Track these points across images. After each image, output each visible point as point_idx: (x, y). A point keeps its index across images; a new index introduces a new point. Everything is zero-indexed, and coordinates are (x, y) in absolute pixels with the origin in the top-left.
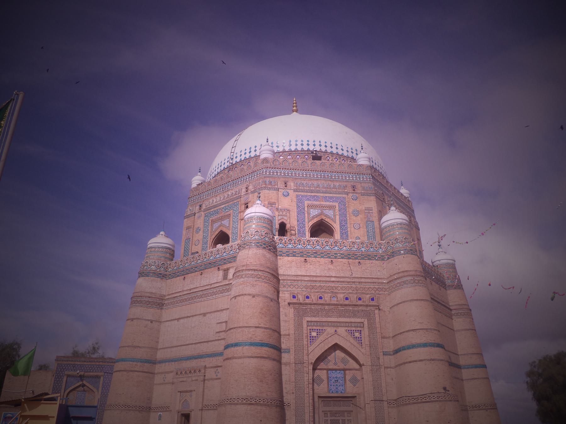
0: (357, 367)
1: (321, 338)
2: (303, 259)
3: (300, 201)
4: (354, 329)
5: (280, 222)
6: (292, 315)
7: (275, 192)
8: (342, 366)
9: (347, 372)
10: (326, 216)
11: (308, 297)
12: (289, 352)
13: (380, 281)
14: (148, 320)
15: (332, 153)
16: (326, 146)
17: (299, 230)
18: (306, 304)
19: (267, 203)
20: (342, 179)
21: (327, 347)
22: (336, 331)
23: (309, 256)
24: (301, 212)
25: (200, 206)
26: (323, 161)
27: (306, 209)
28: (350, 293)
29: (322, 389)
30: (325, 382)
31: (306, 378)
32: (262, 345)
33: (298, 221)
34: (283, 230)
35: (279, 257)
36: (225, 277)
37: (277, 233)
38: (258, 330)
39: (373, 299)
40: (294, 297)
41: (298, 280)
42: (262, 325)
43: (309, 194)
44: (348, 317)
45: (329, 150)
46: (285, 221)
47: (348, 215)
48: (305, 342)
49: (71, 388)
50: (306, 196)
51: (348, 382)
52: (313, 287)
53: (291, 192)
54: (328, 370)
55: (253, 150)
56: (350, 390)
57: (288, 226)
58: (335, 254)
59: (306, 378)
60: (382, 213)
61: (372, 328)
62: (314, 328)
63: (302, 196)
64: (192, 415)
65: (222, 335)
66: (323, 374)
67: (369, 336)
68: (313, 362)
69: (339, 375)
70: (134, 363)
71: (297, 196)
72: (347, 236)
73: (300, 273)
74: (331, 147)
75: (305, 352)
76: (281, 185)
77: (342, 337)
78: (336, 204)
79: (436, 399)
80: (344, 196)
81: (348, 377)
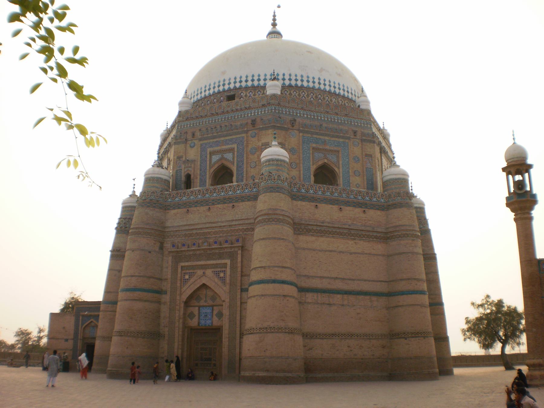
1: (192, 280)
2: (185, 210)
3: (203, 149)
4: (219, 269)
5: (186, 173)
6: (170, 263)
7: (183, 145)
8: (210, 302)
9: (215, 308)
10: (226, 159)
11: (184, 245)
12: (166, 293)
13: (249, 221)
14: (117, 270)
15: (247, 88)
17: (200, 179)
18: (182, 251)
19: (176, 157)
20: (244, 117)
21: (196, 287)
23: (190, 207)
24: (203, 161)
26: (237, 99)
27: (208, 156)
28: (220, 237)
29: (194, 323)
30: (197, 317)
31: (177, 315)
32: (134, 290)
33: (201, 170)
34: (188, 182)
35: (167, 211)
37: (183, 186)
38: (134, 278)
39: (238, 241)
40: (173, 246)
41: (179, 231)
42: (137, 274)
43: (211, 141)
44: (214, 259)
45: (244, 84)
46: (190, 173)
47: (245, 155)
48: (178, 285)
49: (86, 324)
50: (209, 143)
51: (214, 316)
52: (191, 235)
54: (199, 307)
56: (216, 322)
57: (192, 176)
58: (213, 200)
59: (177, 315)
61: (233, 267)
62: (188, 271)
63: (206, 144)
66: (195, 311)
67: (230, 275)
68: (184, 300)
69: (209, 310)
71: (201, 145)
72: (243, 177)
73: (182, 223)
75: (178, 292)
76: (189, 137)
77: (209, 278)
78: (235, 146)
79: (258, 331)
80: (244, 135)
81: (215, 312)
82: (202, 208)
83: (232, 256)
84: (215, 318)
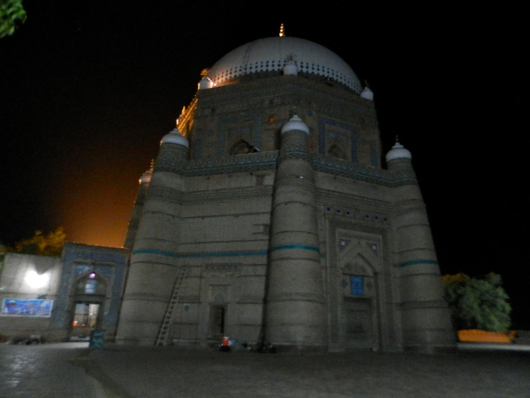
0: (371, 274)
4: (372, 242)
8: (361, 273)
9: (365, 278)
14: (170, 215)
16: (337, 76)
22: (359, 243)
25: (213, 110)
36: (260, 182)
53: (314, 113)
54: (351, 275)
55: (270, 64)
56: (367, 293)
60: (387, 147)
64: (229, 308)
65: (260, 237)
70: (159, 255)
74: (341, 78)
82: (347, 179)
83: (383, 232)
84: (366, 289)
